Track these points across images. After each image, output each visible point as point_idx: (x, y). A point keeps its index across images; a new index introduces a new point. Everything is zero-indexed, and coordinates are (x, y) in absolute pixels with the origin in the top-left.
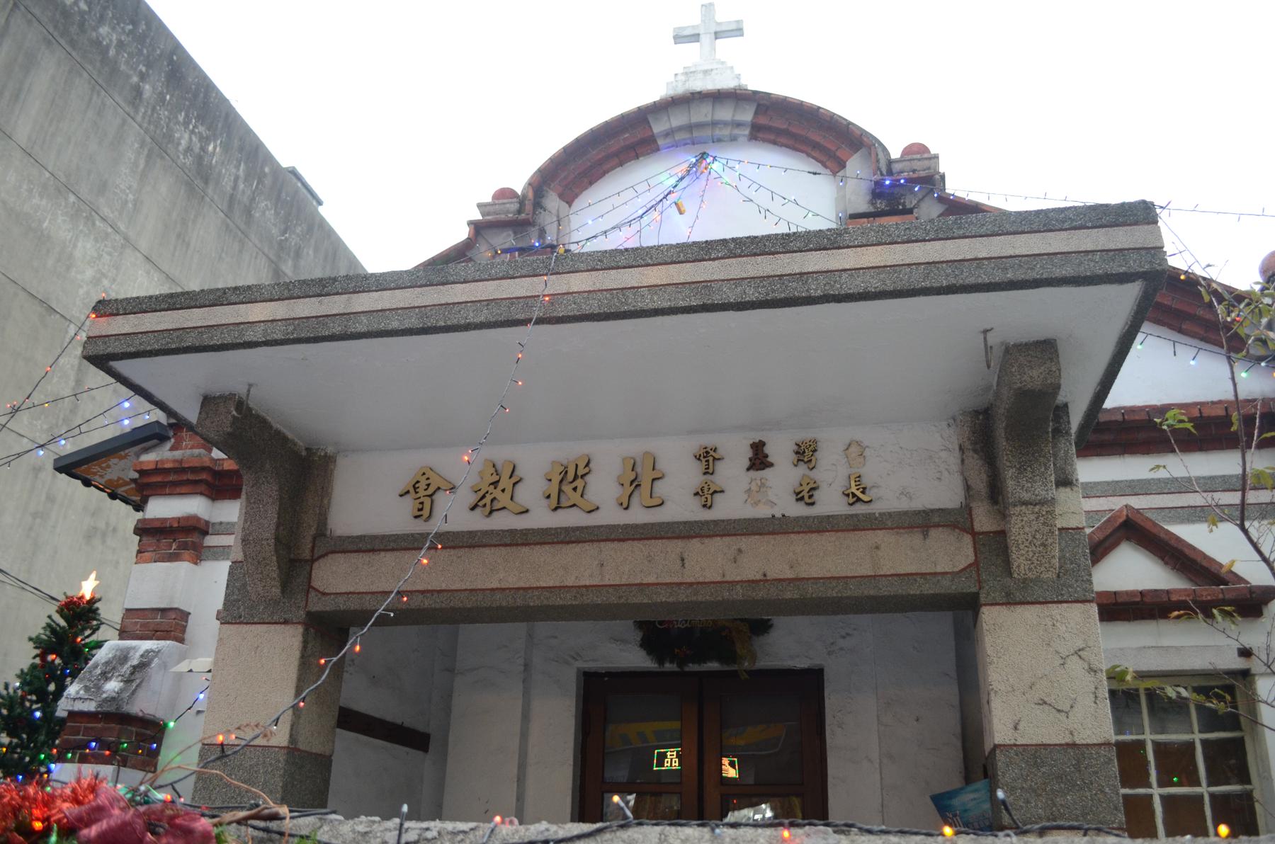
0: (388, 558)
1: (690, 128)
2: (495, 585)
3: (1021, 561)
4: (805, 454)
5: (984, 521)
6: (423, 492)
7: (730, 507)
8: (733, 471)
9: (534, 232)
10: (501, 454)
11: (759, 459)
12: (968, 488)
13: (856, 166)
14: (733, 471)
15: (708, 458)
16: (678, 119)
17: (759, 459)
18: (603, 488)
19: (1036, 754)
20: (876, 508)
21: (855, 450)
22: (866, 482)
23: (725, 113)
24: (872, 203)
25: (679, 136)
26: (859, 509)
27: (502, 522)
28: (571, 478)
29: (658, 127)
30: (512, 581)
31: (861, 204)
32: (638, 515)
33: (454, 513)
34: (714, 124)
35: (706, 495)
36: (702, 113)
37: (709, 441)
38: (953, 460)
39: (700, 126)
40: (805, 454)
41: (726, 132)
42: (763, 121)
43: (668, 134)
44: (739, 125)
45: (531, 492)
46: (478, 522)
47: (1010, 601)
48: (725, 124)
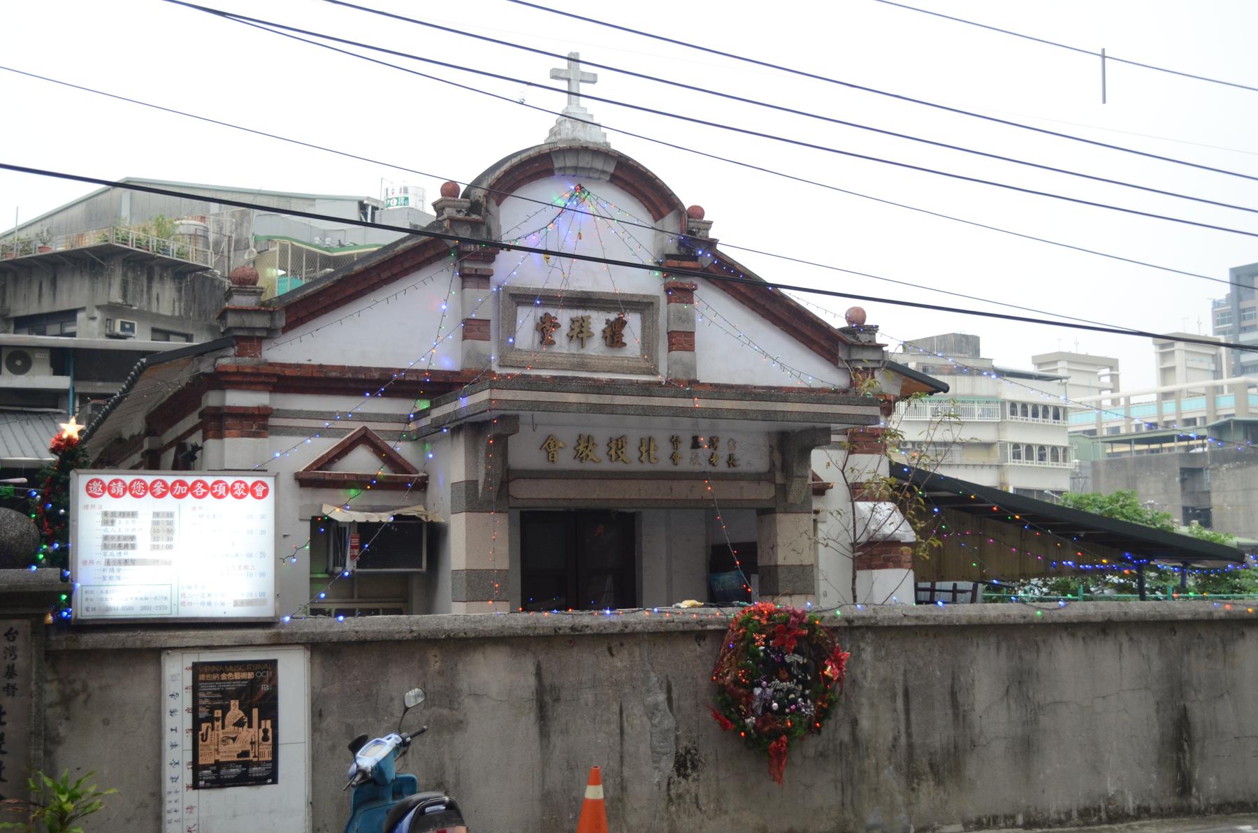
0: (545, 483)
1: (576, 168)
2: (595, 497)
3: (791, 498)
4: (713, 443)
5: (779, 479)
6: (549, 445)
7: (685, 465)
8: (685, 448)
9: (484, 229)
10: (586, 432)
11: (695, 444)
12: (772, 464)
13: (670, 222)
14: (685, 448)
15: (675, 441)
16: (570, 161)
17: (695, 444)
18: (631, 451)
19: (790, 568)
20: (738, 469)
21: (732, 443)
22: (736, 457)
23: (599, 164)
24: (678, 248)
25: (568, 172)
26: (732, 470)
27: (588, 466)
28: (617, 445)
29: (558, 164)
30: (603, 496)
31: (672, 247)
32: (647, 467)
33: (566, 460)
34: (591, 169)
35: (673, 458)
36: (585, 161)
37: (674, 433)
38: (766, 450)
39: (583, 169)
40: (713, 443)
41: (596, 175)
42: (619, 174)
43: (560, 169)
44: (603, 172)
45: (600, 451)
46: (576, 465)
47: (786, 512)
48: (597, 170)
